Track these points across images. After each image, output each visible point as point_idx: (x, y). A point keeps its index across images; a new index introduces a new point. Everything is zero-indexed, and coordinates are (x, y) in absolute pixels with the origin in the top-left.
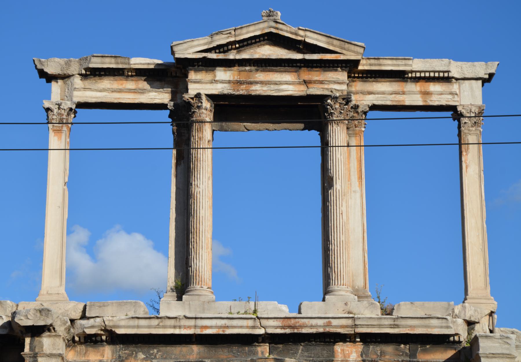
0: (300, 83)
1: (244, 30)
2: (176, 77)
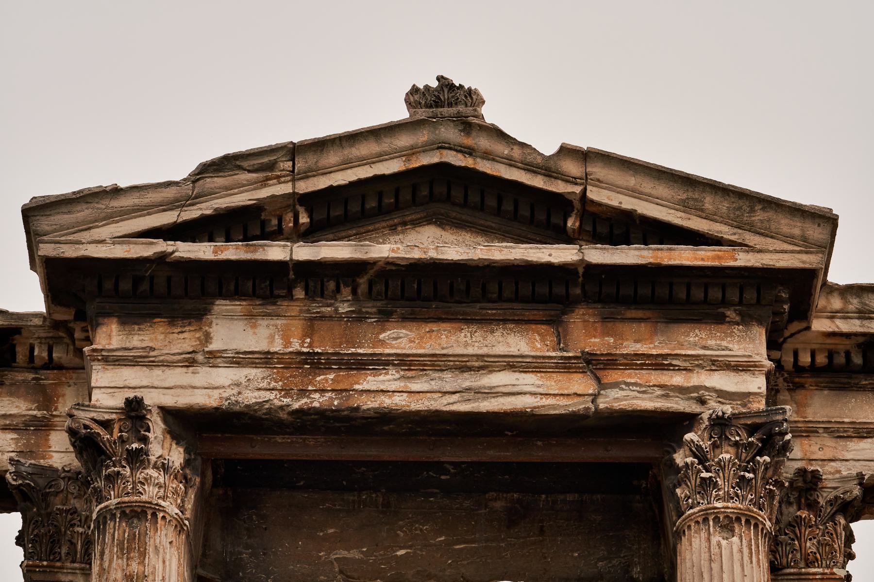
0: (566, 366)
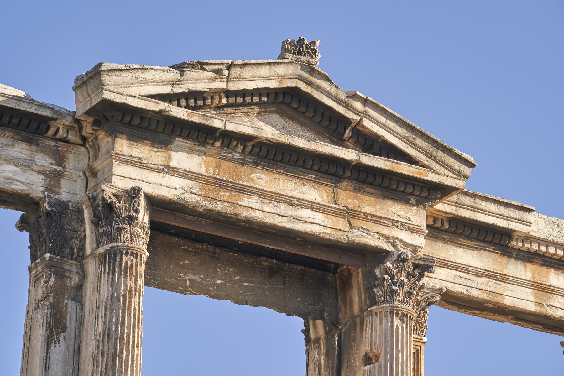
0: (337, 213)
1: (248, 72)
2: (65, 140)
